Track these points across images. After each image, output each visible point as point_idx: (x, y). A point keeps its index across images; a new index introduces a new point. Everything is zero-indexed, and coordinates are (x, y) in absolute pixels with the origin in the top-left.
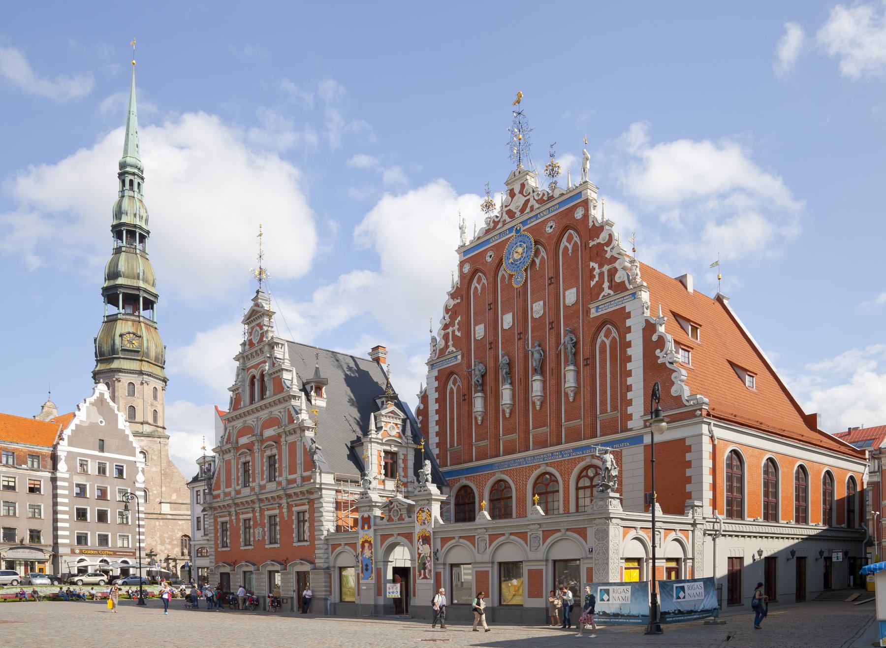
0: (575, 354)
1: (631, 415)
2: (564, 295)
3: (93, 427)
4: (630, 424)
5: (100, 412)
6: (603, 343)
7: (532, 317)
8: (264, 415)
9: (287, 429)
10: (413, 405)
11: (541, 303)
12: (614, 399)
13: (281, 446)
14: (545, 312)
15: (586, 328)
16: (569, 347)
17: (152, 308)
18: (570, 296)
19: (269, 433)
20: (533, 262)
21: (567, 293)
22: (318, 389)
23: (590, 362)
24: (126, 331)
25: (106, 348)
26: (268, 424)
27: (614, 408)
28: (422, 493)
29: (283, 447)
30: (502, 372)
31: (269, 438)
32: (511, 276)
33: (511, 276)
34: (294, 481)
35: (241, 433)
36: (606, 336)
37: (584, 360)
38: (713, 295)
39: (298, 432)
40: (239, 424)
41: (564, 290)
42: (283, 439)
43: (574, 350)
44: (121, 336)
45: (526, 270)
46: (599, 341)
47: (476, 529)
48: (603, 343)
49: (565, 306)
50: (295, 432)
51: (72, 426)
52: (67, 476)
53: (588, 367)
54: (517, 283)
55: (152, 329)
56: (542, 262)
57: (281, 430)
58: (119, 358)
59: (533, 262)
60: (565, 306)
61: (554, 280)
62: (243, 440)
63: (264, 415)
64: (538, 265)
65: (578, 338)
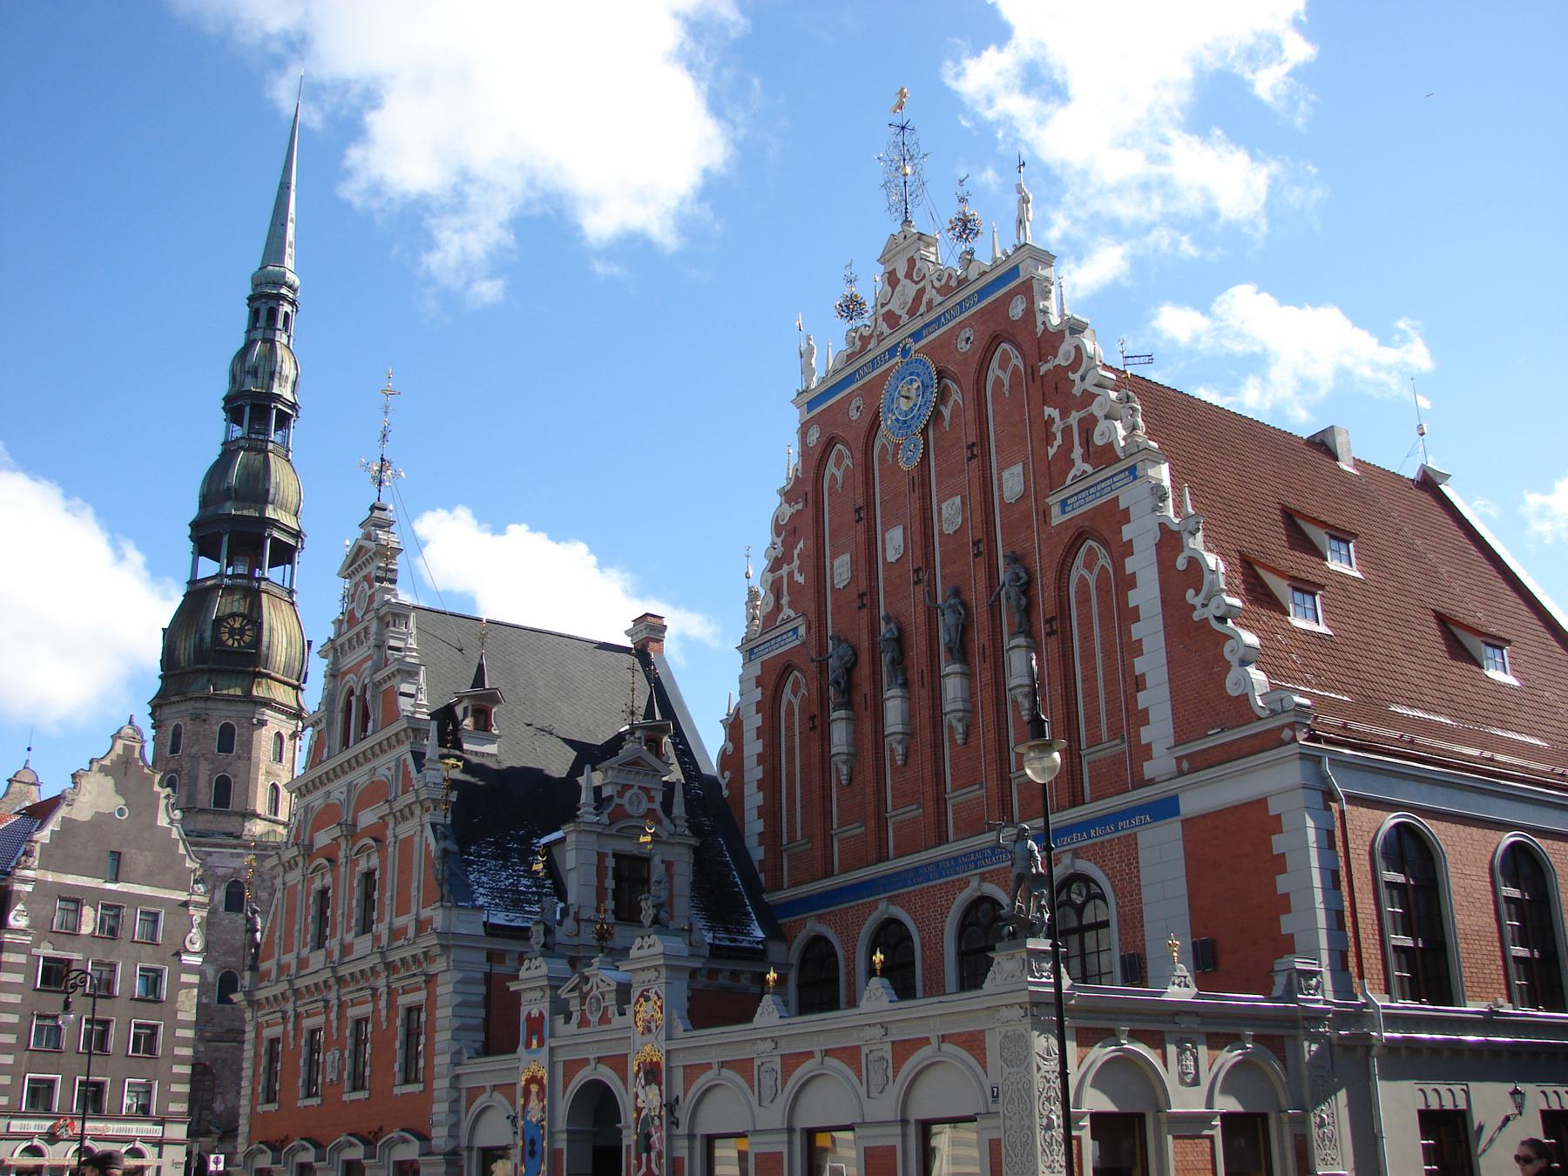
0: (1028, 610)
1: (1149, 746)
2: (1000, 479)
3: (100, 820)
4: (1149, 769)
5: (120, 790)
6: (1083, 581)
7: (941, 532)
8: (361, 777)
9: (398, 806)
10: (711, 741)
11: (958, 500)
12: (1112, 711)
13: (385, 848)
14: (964, 521)
15: (1044, 551)
17: (291, 561)
18: (1012, 482)
19: (367, 818)
20: (937, 415)
22: (483, 718)
23: (1059, 623)
24: (228, 612)
25: (185, 650)
27: (1115, 733)
28: (645, 952)
29: (391, 849)
30: (886, 659)
31: (368, 831)
32: (897, 446)
33: (897, 446)
34: (404, 930)
35: (320, 821)
36: (1088, 566)
37: (1046, 621)
38: (1411, 472)
39: (418, 811)
41: (1001, 469)
42: (389, 833)
43: (1023, 601)
44: (219, 621)
45: (924, 432)
49: (1003, 504)
50: (412, 814)
51: (53, 825)
52: (27, 939)
53: (1054, 638)
54: (907, 461)
55: (285, 607)
57: (385, 809)
58: (211, 671)
59: (937, 415)
60: (1003, 504)
61: (979, 450)
62: (322, 839)
63: (361, 777)
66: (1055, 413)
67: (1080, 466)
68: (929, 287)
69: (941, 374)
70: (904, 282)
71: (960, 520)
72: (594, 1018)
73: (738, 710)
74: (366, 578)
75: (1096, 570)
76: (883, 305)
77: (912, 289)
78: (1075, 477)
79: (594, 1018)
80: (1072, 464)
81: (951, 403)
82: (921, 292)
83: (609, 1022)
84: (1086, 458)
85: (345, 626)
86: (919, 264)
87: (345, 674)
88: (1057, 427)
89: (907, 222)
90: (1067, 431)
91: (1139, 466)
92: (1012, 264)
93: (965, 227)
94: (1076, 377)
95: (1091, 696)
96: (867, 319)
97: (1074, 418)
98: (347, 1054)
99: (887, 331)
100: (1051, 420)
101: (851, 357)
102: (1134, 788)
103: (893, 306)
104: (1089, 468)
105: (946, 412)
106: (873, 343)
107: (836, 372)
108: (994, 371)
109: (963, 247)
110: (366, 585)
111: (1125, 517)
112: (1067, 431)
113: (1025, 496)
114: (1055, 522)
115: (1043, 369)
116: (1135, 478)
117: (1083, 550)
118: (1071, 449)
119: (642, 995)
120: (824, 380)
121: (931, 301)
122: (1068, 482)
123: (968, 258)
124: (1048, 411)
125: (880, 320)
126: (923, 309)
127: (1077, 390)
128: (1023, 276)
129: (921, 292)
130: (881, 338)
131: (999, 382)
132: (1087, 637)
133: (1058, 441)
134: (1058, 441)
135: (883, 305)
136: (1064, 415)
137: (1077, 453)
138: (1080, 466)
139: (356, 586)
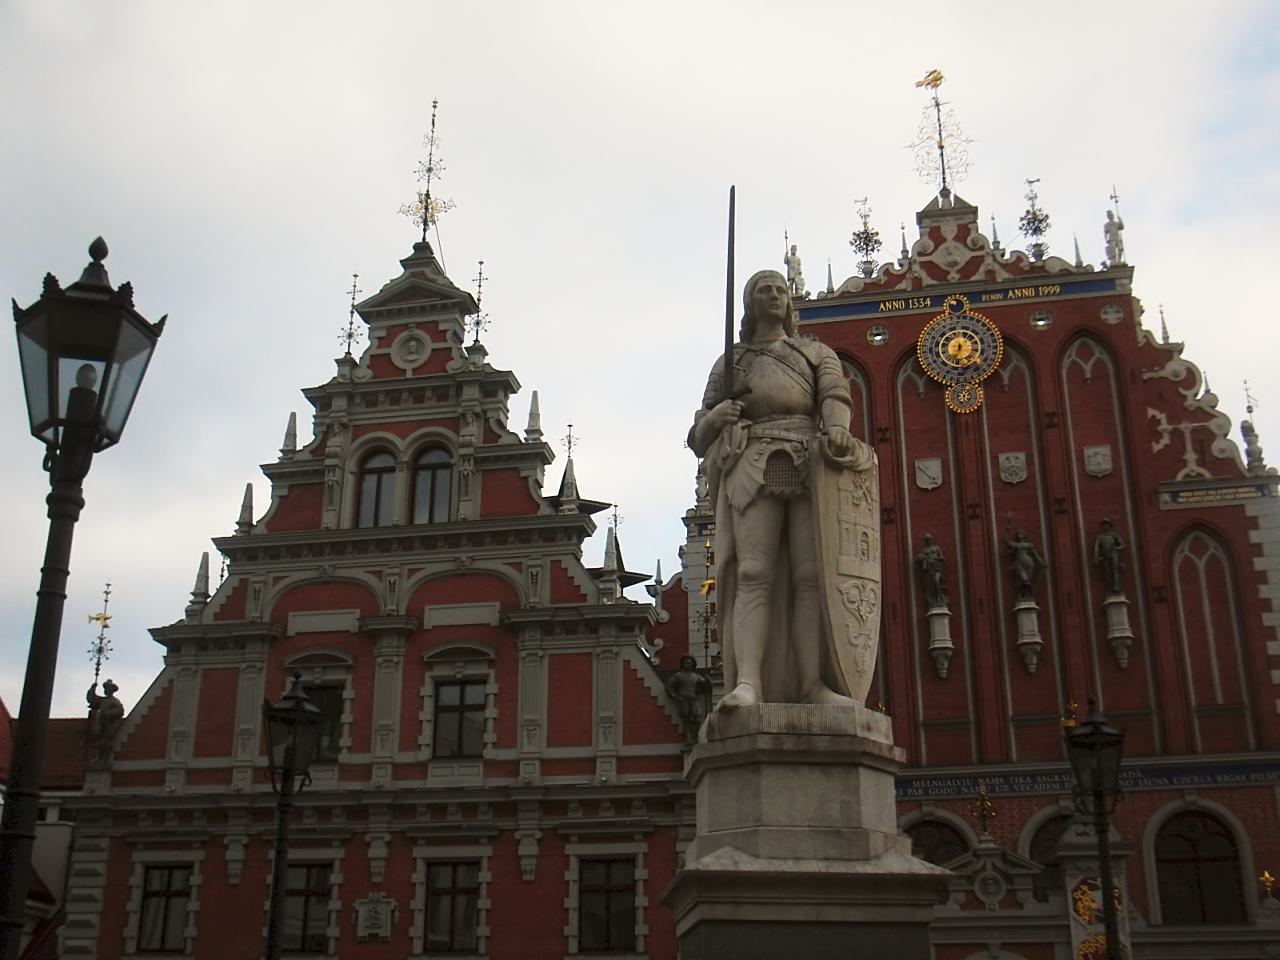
7: (997, 478)
11: (1022, 456)
14: (1031, 476)
16: (1115, 556)
21: (1088, 451)
23: (1159, 594)
26: (436, 589)
32: (937, 388)
33: (937, 388)
40: (299, 572)
46: (1178, 558)
47: (1266, 943)
48: (1188, 567)
49: (1086, 476)
56: (1017, 375)
61: (1050, 421)
64: (1006, 382)
65: (1128, 542)
66: (1162, 417)
67: (1192, 466)
68: (989, 260)
69: (1007, 340)
70: (950, 243)
71: (1024, 475)
72: (992, 901)
73: (677, 580)
74: (419, 325)
75: (1205, 558)
76: (920, 254)
77: (963, 256)
78: (1187, 476)
79: (992, 901)
80: (1184, 464)
81: (1010, 368)
82: (981, 259)
83: (1021, 906)
84: (1201, 463)
85: (365, 374)
86: (973, 235)
87: (358, 431)
88: (1164, 426)
89: (945, 192)
90: (1177, 435)
91: (1272, 486)
92: (1110, 276)
93: (1035, 223)
94: (1189, 393)
95: (1201, 662)
96: (888, 255)
97: (1186, 427)
98: (418, 902)
99: (927, 280)
100: (1156, 421)
101: (871, 287)
102: (1260, 747)
103: (936, 258)
104: (1207, 475)
105: (1006, 376)
106: (902, 286)
107: (845, 294)
108: (1071, 356)
109: (1034, 240)
110: (426, 338)
111: (1254, 523)
112: (1177, 435)
113: (1114, 474)
114: (1163, 507)
115: (1145, 377)
116: (1264, 495)
117: (1190, 537)
118: (1184, 450)
119: (1084, 882)
120: (822, 298)
121: (990, 273)
122: (1180, 477)
123: (1038, 250)
124: (1151, 412)
125: (916, 267)
126: (979, 276)
127: (1189, 402)
128: (1119, 291)
129: (974, 264)
130: (917, 281)
131: (1075, 368)
132: (1194, 612)
133: (1166, 440)
134: (1166, 440)
135: (920, 254)
136: (1170, 420)
137: (1191, 456)
138: (1192, 466)
139: (393, 332)
